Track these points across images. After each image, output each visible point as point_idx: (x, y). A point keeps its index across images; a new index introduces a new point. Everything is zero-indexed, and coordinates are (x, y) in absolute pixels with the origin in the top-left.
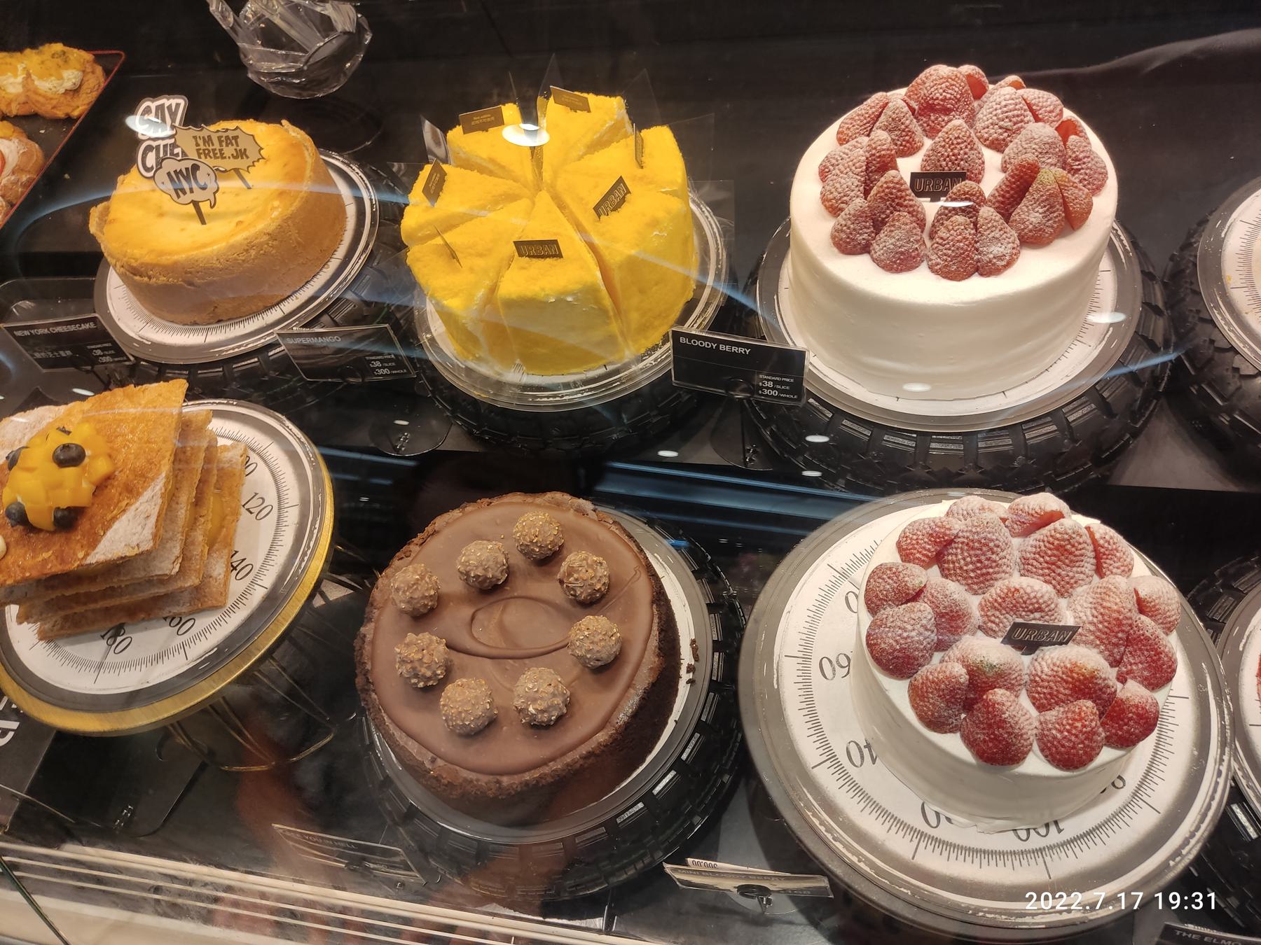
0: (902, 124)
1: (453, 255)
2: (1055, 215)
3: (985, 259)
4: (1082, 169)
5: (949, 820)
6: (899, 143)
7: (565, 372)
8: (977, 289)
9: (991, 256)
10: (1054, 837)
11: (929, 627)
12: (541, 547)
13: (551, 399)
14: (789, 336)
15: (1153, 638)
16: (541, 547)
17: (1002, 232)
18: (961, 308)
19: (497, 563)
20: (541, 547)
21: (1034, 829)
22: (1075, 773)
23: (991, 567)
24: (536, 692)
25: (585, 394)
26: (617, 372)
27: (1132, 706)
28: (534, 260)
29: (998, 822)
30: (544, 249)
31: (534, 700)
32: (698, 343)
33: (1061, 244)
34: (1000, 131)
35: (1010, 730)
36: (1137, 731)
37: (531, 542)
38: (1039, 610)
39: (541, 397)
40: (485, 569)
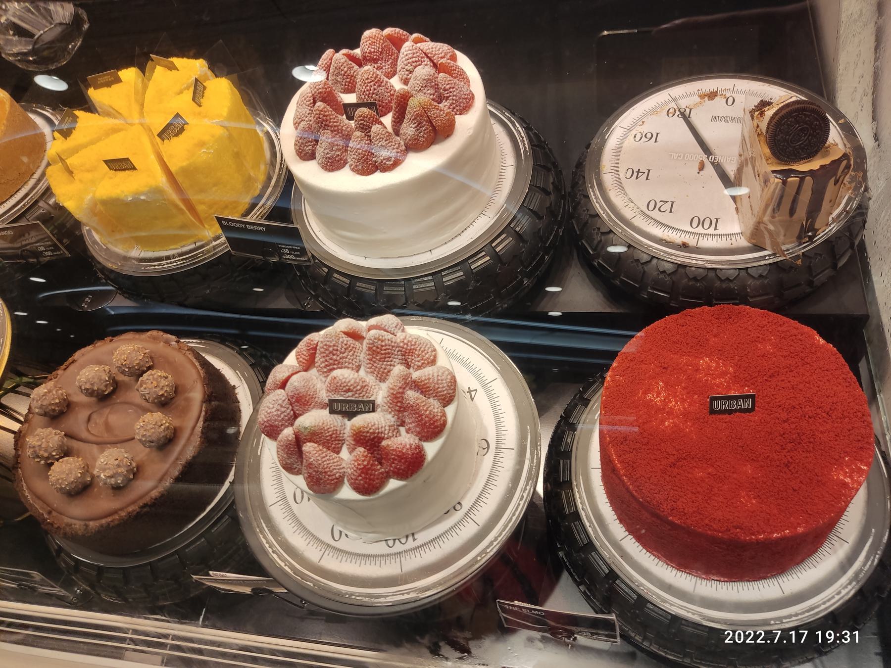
0: (342, 70)
1: (71, 173)
2: (424, 128)
3: (379, 160)
4: (450, 96)
5: (346, 535)
6: (343, 83)
7: (167, 248)
8: (378, 180)
9: (382, 158)
10: (410, 544)
11: (284, 405)
12: (129, 368)
13: (156, 267)
14: (307, 218)
15: (414, 405)
16: (129, 368)
17: (387, 142)
18: (362, 194)
19: (101, 380)
20: (129, 368)
21: (399, 539)
22: (371, 497)
23: (334, 364)
24: (106, 464)
25: (179, 263)
26: (202, 246)
27: (392, 450)
28: (119, 172)
29: (371, 535)
30: (120, 165)
31: (104, 470)
32: (233, 224)
33: (435, 148)
34: (407, 73)
35: (316, 469)
36: (403, 467)
37: (122, 364)
38: (349, 390)
39: (150, 266)
40: (92, 384)
